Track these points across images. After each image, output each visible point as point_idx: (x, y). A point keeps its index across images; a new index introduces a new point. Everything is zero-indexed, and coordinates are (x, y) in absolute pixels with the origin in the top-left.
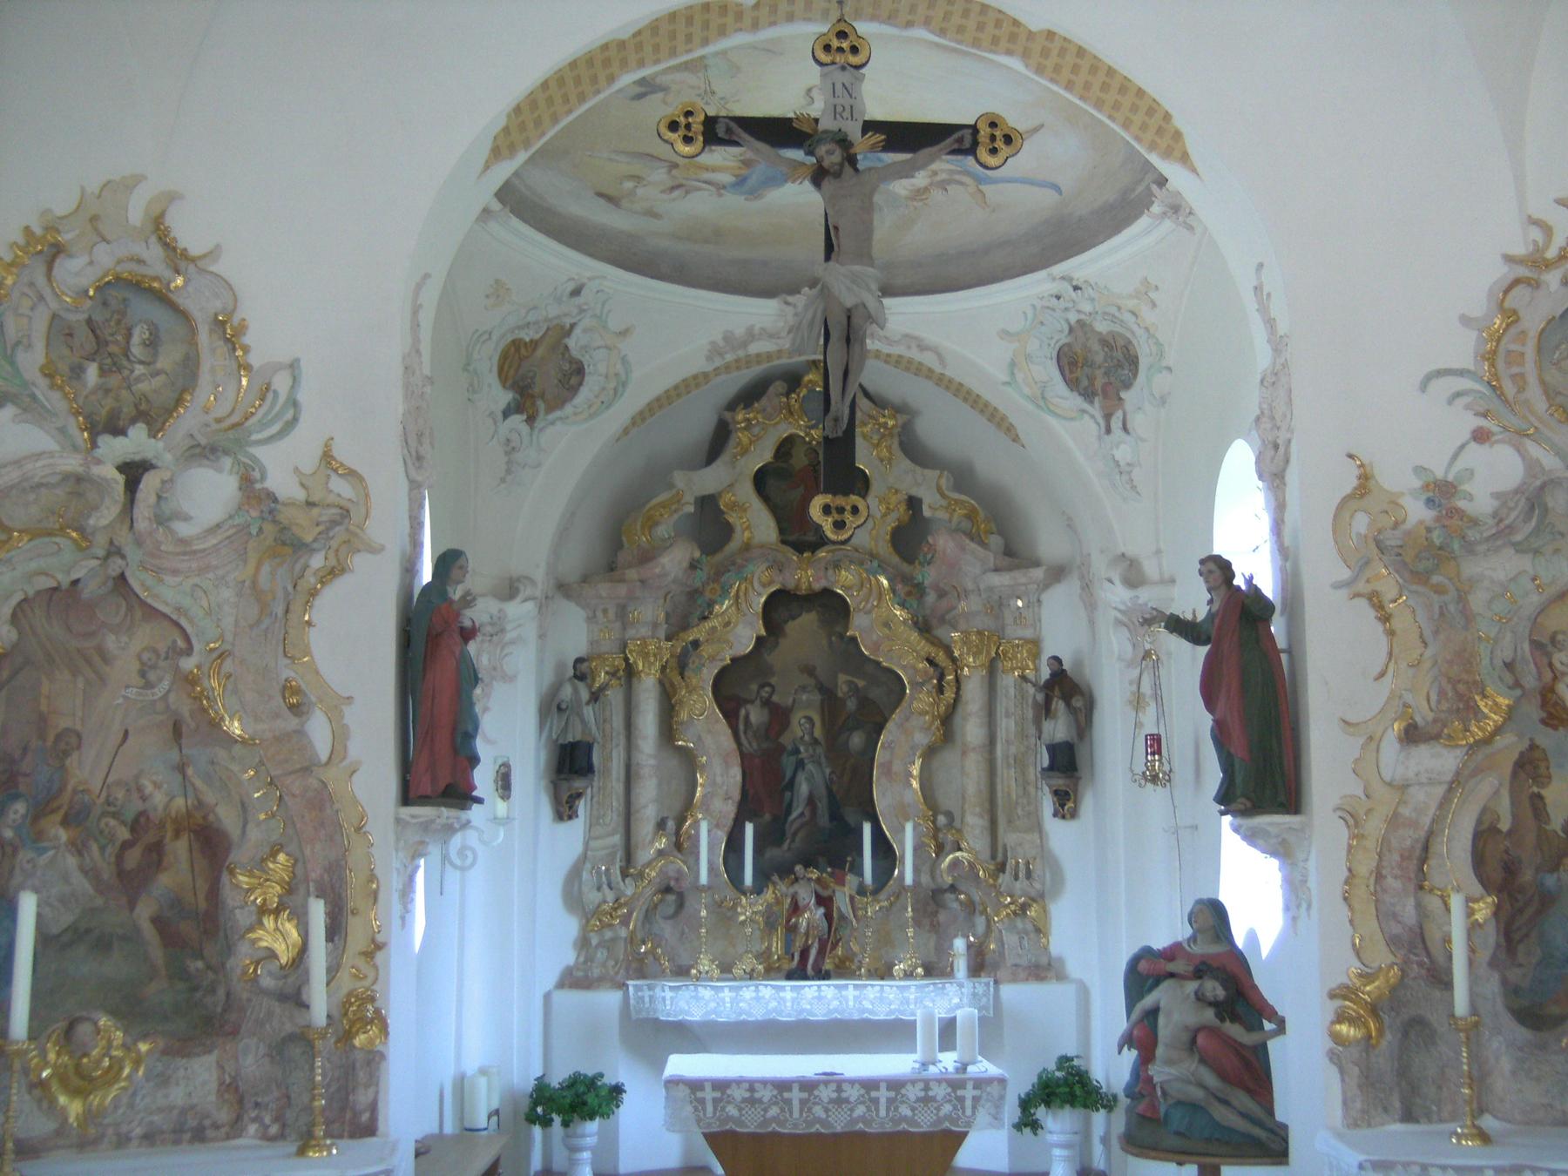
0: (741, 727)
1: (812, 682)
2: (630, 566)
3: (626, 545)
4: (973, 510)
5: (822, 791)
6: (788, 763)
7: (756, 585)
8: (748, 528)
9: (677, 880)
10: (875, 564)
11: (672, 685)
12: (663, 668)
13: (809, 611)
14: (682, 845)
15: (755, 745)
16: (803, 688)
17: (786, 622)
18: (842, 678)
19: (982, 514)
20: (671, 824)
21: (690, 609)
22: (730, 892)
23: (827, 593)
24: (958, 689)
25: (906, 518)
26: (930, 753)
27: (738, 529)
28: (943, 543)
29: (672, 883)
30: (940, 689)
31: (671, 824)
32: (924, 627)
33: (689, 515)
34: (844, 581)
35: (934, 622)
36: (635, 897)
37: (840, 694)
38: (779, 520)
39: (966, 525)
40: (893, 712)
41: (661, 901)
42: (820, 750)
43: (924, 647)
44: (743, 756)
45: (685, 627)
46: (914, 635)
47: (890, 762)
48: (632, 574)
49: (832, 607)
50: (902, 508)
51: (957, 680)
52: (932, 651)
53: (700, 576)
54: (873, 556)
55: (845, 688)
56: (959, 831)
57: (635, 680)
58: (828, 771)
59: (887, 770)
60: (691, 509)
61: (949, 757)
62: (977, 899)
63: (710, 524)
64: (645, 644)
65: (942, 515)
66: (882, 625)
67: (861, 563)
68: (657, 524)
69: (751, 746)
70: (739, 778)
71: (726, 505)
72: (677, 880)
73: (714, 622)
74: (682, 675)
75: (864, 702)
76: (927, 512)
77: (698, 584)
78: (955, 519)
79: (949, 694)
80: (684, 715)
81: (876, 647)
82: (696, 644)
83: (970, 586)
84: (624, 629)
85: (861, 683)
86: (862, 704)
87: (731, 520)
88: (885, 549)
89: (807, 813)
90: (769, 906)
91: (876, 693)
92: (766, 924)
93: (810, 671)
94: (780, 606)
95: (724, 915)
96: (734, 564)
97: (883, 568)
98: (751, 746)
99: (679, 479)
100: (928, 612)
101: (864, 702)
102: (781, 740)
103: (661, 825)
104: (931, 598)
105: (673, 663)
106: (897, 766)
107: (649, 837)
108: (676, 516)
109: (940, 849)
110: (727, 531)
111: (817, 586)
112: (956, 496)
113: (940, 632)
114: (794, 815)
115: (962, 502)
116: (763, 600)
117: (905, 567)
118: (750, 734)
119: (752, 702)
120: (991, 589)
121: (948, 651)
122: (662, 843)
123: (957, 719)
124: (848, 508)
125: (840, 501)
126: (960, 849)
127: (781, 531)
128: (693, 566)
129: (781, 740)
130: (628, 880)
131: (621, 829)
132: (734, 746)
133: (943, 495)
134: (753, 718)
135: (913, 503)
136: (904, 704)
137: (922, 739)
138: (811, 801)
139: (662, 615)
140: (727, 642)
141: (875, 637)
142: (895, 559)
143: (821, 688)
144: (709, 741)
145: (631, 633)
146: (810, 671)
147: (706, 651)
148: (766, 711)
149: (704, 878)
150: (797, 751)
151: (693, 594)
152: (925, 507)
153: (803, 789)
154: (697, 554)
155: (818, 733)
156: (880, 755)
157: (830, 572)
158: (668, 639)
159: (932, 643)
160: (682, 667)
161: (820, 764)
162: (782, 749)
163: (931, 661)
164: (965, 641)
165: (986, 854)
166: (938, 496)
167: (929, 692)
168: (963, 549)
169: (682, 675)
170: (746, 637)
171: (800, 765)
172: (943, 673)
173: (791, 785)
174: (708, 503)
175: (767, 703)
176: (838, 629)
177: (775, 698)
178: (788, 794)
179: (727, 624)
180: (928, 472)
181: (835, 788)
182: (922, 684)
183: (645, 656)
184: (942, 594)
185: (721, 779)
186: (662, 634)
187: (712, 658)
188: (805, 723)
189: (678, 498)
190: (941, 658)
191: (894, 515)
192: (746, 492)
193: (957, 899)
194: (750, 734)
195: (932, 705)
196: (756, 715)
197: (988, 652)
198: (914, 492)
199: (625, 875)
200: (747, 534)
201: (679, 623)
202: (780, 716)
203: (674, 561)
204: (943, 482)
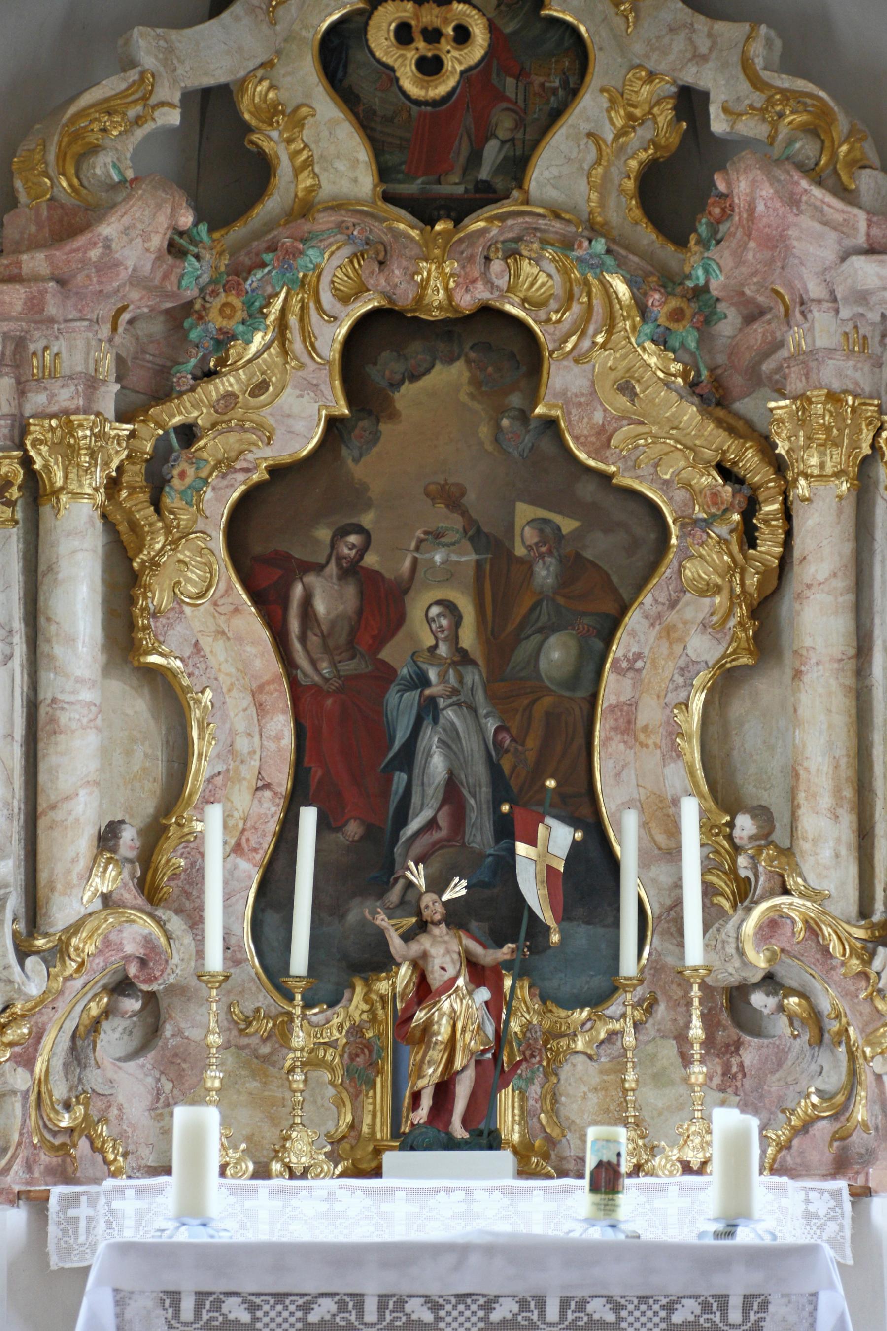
0: (294, 626)
1: (456, 522)
2: (34, 245)
3: (23, 198)
4: (824, 113)
5: (478, 772)
6: (401, 707)
7: (326, 298)
8: (308, 163)
9: (143, 962)
10: (600, 246)
11: (134, 526)
12: (113, 485)
13: (451, 360)
14: (157, 874)
15: (325, 667)
16: (436, 536)
17: (396, 386)
18: (525, 512)
19: (842, 124)
20: (129, 837)
21: (171, 358)
22: (265, 999)
23: (488, 313)
24: (789, 534)
25: (674, 140)
26: (726, 682)
27: (284, 168)
28: (748, 187)
29: (132, 970)
30: (749, 536)
31: (129, 837)
32: (713, 394)
33: (169, 131)
34: (528, 287)
35: (736, 381)
36: (46, 1000)
37: (520, 551)
38: (378, 148)
39: (805, 147)
40: (639, 587)
41: (107, 1013)
42: (472, 677)
43: (714, 440)
44: (294, 685)
45: (163, 392)
46: (690, 412)
47: (633, 705)
48: (35, 262)
49: (503, 347)
50: (665, 115)
51: (787, 514)
52: (731, 447)
53: (194, 274)
54: (594, 229)
55: (530, 535)
56: (788, 853)
57: (46, 510)
58: (491, 725)
59: (627, 726)
60: (173, 117)
61: (766, 688)
62: (825, 1005)
63: (222, 159)
64: (70, 428)
65: (751, 128)
66: (616, 391)
67: (567, 244)
68: (95, 149)
69: (316, 669)
70: (288, 740)
71: (257, 111)
72: (143, 962)
73: (228, 383)
74: (156, 503)
75: (574, 565)
76: (718, 125)
77: (190, 292)
78: (783, 131)
79: (769, 547)
80: (159, 596)
81: (602, 440)
82: (188, 434)
83: (815, 289)
84: (21, 392)
85: (568, 525)
86: (576, 568)
87: (267, 146)
88: (623, 212)
89: (443, 821)
90: (356, 1030)
91: (599, 547)
92: (349, 1072)
93: (451, 497)
94: (380, 344)
95: (258, 1049)
96: (272, 248)
97: (619, 252)
98: (316, 669)
99: (145, 45)
100: (721, 359)
101: (574, 565)
102: (385, 654)
103: (107, 838)
104: (728, 325)
105: (135, 474)
106: (649, 713)
107: (82, 864)
108: (140, 133)
109: (744, 894)
110: (262, 169)
111: (466, 301)
112: (785, 82)
113: (745, 406)
114: (414, 825)
115: (799, 95)
116: (343, 331)
117: (668, 252)
118: (314, 640)
119: (319, 568)
120: (862, 297)
121: (766, 446)
122: (107, 880)
123: (786, 607)
124: (450, 30)
125: (431, 16)
126: (786, 892)
127: (384, 173)
128: (175, 249)
129: (385, 654)
130: (30, 961)
131: (16, 848)
132: (277, 668)
133: (756, 83)
134: (320, 607)
135: (690, 103)
136: (667, 570)
137: (704, 649)
138: (452, 793)
139: (109, 362)
140: (260, 427)
141: (598, 417)
142: (647, 235)
143: (477, 536)
144: (218, 653)
145: (37, 400)
146: (451, 497)
147: (210, 446)
148: (350, 590)
149: (215, 960)
150: (425, 682)
151: (181, 316)
152: (714, 110)
153: (437, 765)
154: (186, 219)
155: (468, 637)
156: (613, 689)
157: (497, 265)
158: (122, 418)
159: (731, 430)
160: (157, 487)
161: (473, 710)
162: (385, 675)
163: (726, 472)
164: (802, 421)
165: (847, 900)
166: (744, 86)
167: (722, 541)
168: (793, 201)
169: (156, 503)
170: (299, 417)
171: (429, 710)
172: (753, 505)
173: (407, 757)
174: (213, 105)
175: (352, 570)
176: (516, 400)
177: (371, 560)
178: (400, 779)
179: (261, 387)
180: (720, 26)
181: (506, 764)
182: (707, 523)
183: (68, 451)
184: (753, 315)
185: (247, 736)
186: (108, 399)
187: (226, 465)
188: (438, 617)
189: (143, 92)
190: (750, 461)
191: (645, 133)
192: (304, 78)
193: (781, 1008)
194: (314, 640)
195: (730, 571)
196: (328, 598)
197: (855, 445)
198: (690, 76)
199: (22, 954)
200: (306, 181)
201: (148, 389)
202: (382, 603)
203: (135, 236)
204: (758, 51)
